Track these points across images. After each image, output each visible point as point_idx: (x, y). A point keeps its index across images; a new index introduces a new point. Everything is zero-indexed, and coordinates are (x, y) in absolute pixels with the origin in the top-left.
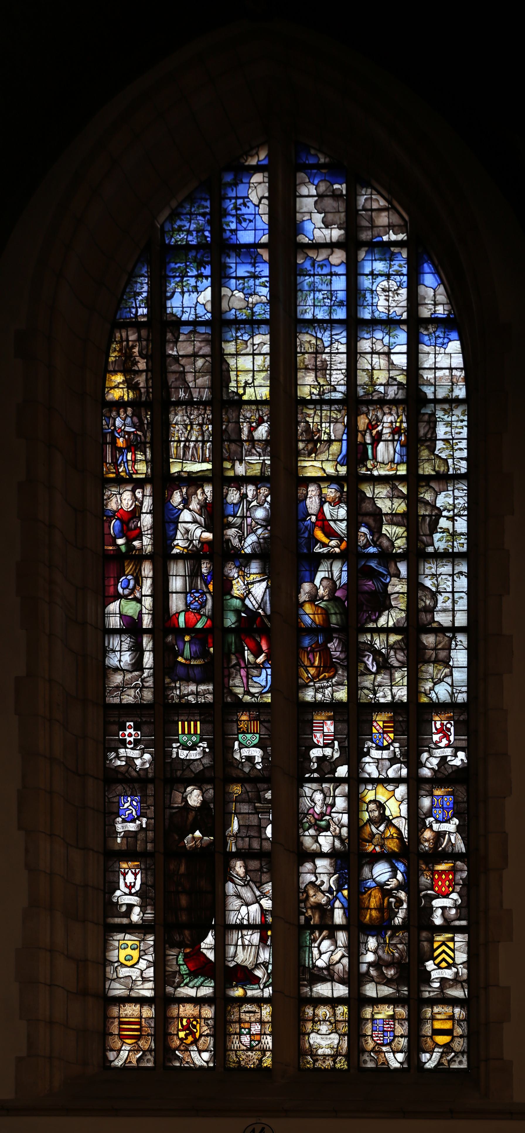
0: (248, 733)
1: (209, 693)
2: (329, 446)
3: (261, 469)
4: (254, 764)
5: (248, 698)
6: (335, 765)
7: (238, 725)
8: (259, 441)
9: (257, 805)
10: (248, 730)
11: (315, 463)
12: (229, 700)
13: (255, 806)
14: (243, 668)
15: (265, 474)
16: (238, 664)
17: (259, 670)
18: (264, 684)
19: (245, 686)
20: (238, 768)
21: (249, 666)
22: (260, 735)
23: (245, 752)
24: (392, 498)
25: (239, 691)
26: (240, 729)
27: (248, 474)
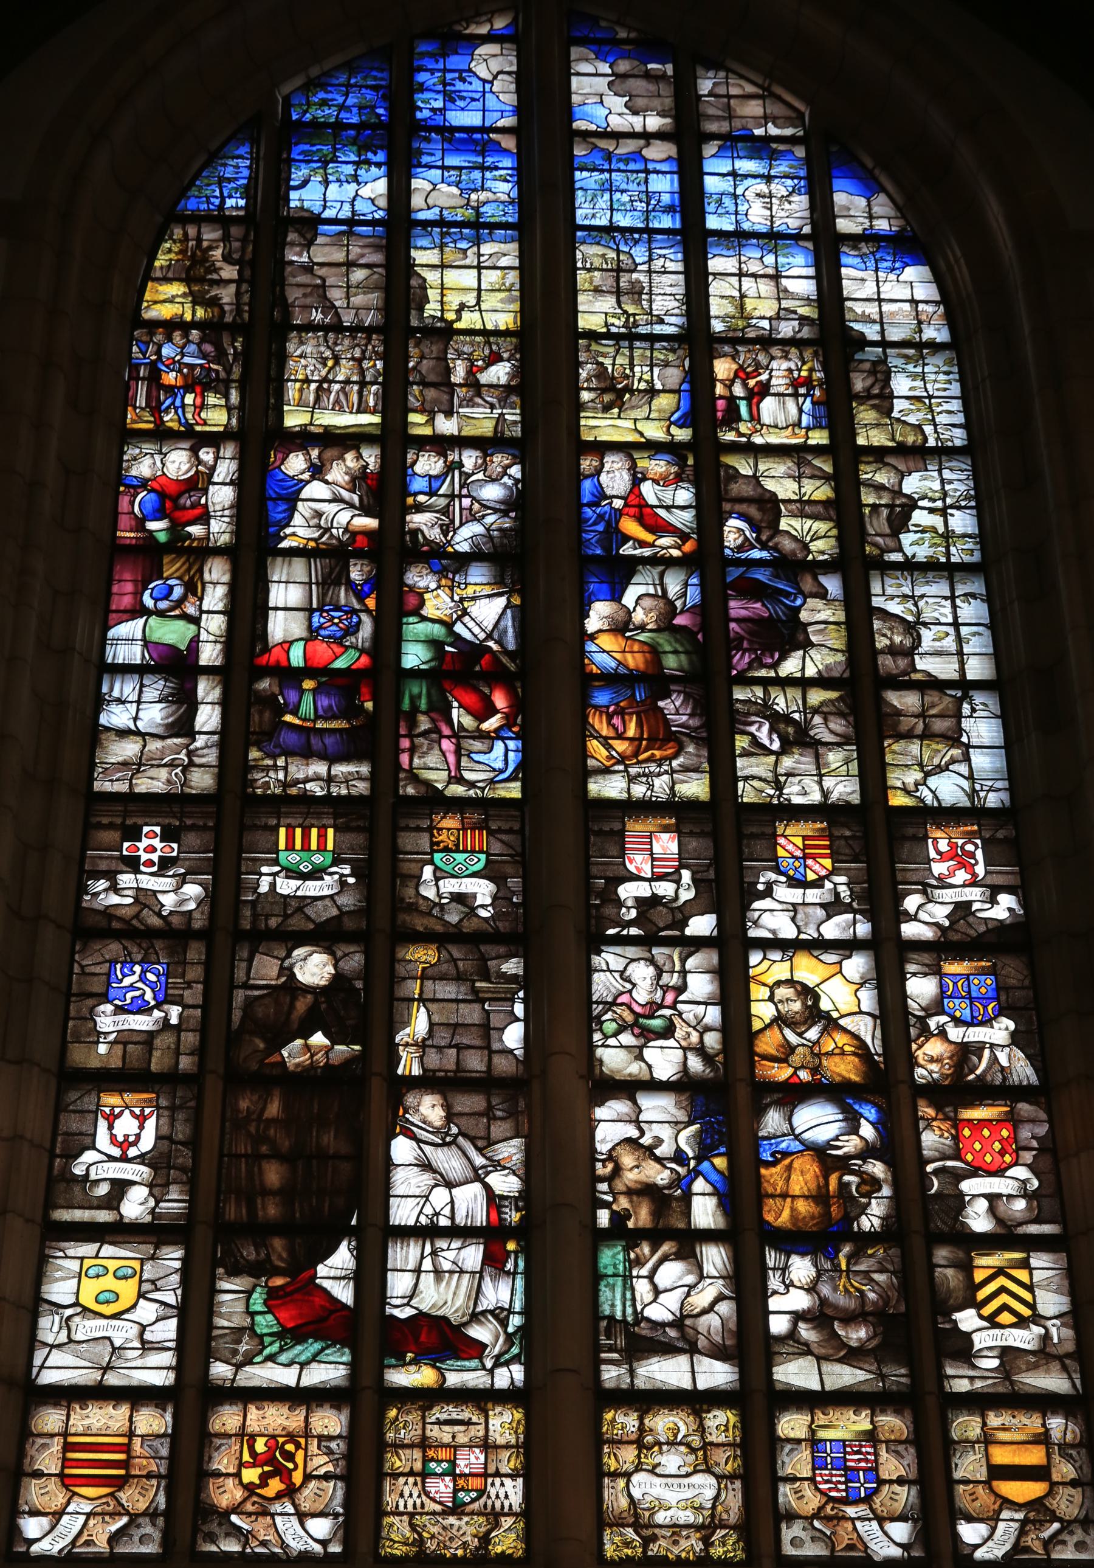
0: (457, 851)
1: (360, 779)
2: (652, 399)
3: (496, 427)
4: (473, 909)
5: (458, 790)
6: (681, 915)
7: (432, 836)
8: (491, 386)
9: (478, 984)
10: (457, 845)
11: (618, 422)
12: (411, 790)
13: (473, 987)
14: (448, 737)
15: (503, 433)
16: (436, 730)
17: (487, 741)
18: (499, 765)
19: (452, 768)
20: (429, 914)
21: (459, 735)
22: (488, 854)
23: (449, 886)
24: (800, 477)
25: (438, 778)
26: (438, 843)
27: (463, 433)
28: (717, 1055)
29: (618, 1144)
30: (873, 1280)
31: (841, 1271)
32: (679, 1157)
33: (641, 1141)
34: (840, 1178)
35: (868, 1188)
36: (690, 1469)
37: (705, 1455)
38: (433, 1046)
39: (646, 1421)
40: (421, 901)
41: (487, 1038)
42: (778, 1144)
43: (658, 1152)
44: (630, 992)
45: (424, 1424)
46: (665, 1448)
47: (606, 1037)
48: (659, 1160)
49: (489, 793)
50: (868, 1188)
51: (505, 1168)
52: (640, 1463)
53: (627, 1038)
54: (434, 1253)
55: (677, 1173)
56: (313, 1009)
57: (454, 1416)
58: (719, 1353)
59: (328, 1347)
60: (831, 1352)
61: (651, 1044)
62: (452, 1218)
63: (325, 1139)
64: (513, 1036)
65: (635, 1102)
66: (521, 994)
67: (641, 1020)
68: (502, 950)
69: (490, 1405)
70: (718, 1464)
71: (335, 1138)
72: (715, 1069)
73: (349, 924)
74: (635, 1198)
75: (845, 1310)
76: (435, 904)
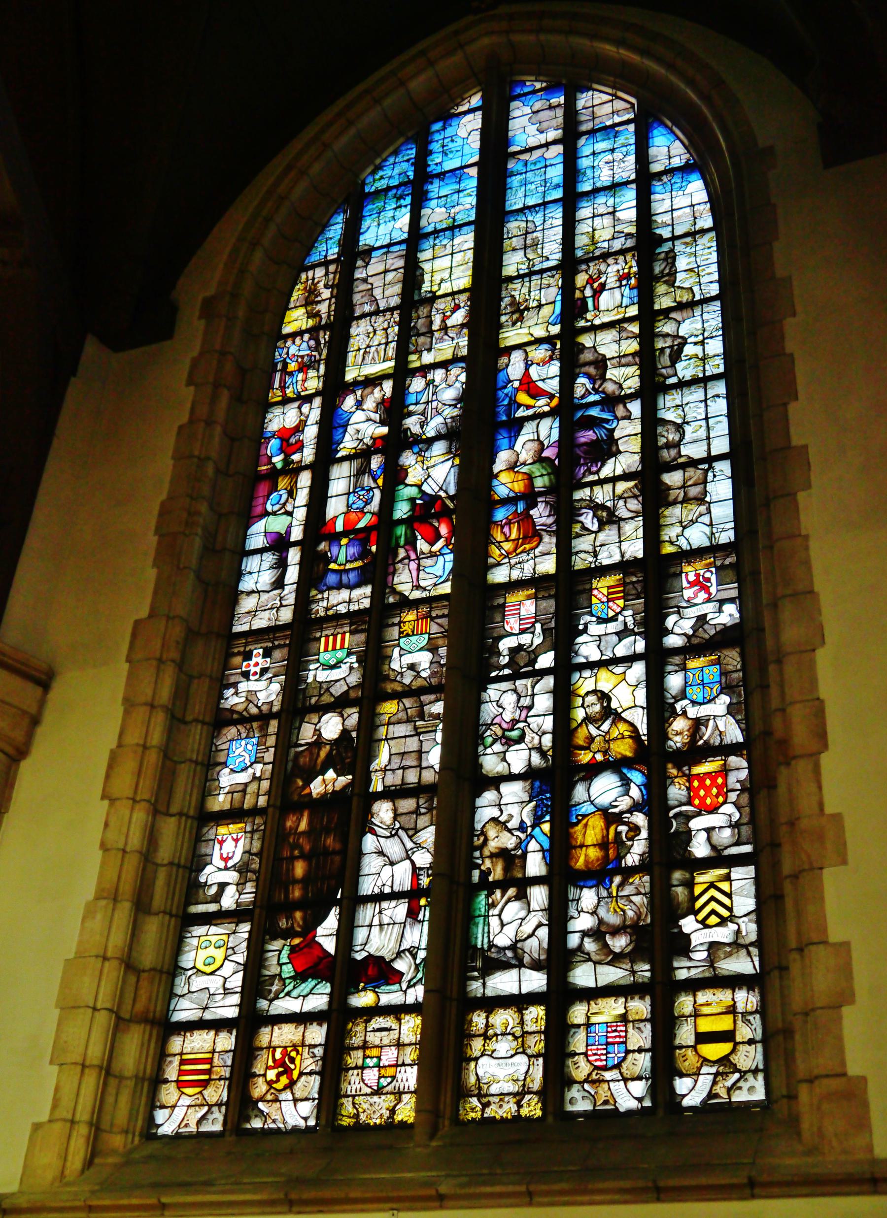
28: (548, 751)
29: (486, 823)
30: (631, 901)
31: (613, 897)
32: (522, 827)
33: (500, 819)
34: (616, 829)
35: (632, 834)
36: (513, 1052)
37: (523, 1041)
38: (390, 770)
39: (490, 1019)
40: (391, 673)
41: (420, 759)
42: (580, 809)
43: (509, 825)
44: (501, 714)
45: (366, 1032)
46: (500, 1037)
47: (486, 748)
48: (510, 831)
49: (433, 593)
50: (632, 834)
51: (423, 848)
52: (485, 1050)
53: (498, 747)
54: (380, 912)
55: (520, 838)
56: (329, 755)
57: (383, 1026)
58: (536, 966)
59: (319, 983)
60: (603, 957)
61: (511, 749)
62: (392, 887)
63: (328, 841)
64: (434, 757)
65: (499, 792)
66: (441, 726)
67: (507, 733)
68: (432, 697)
69: (403, 1016)
70: (529, 1047)
71: (334, 839)
72: (547, 761)
73: (352, 694)
74: (494, 859)
75: (613, 926)
76: (399, 673)
